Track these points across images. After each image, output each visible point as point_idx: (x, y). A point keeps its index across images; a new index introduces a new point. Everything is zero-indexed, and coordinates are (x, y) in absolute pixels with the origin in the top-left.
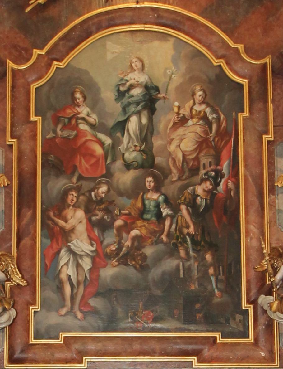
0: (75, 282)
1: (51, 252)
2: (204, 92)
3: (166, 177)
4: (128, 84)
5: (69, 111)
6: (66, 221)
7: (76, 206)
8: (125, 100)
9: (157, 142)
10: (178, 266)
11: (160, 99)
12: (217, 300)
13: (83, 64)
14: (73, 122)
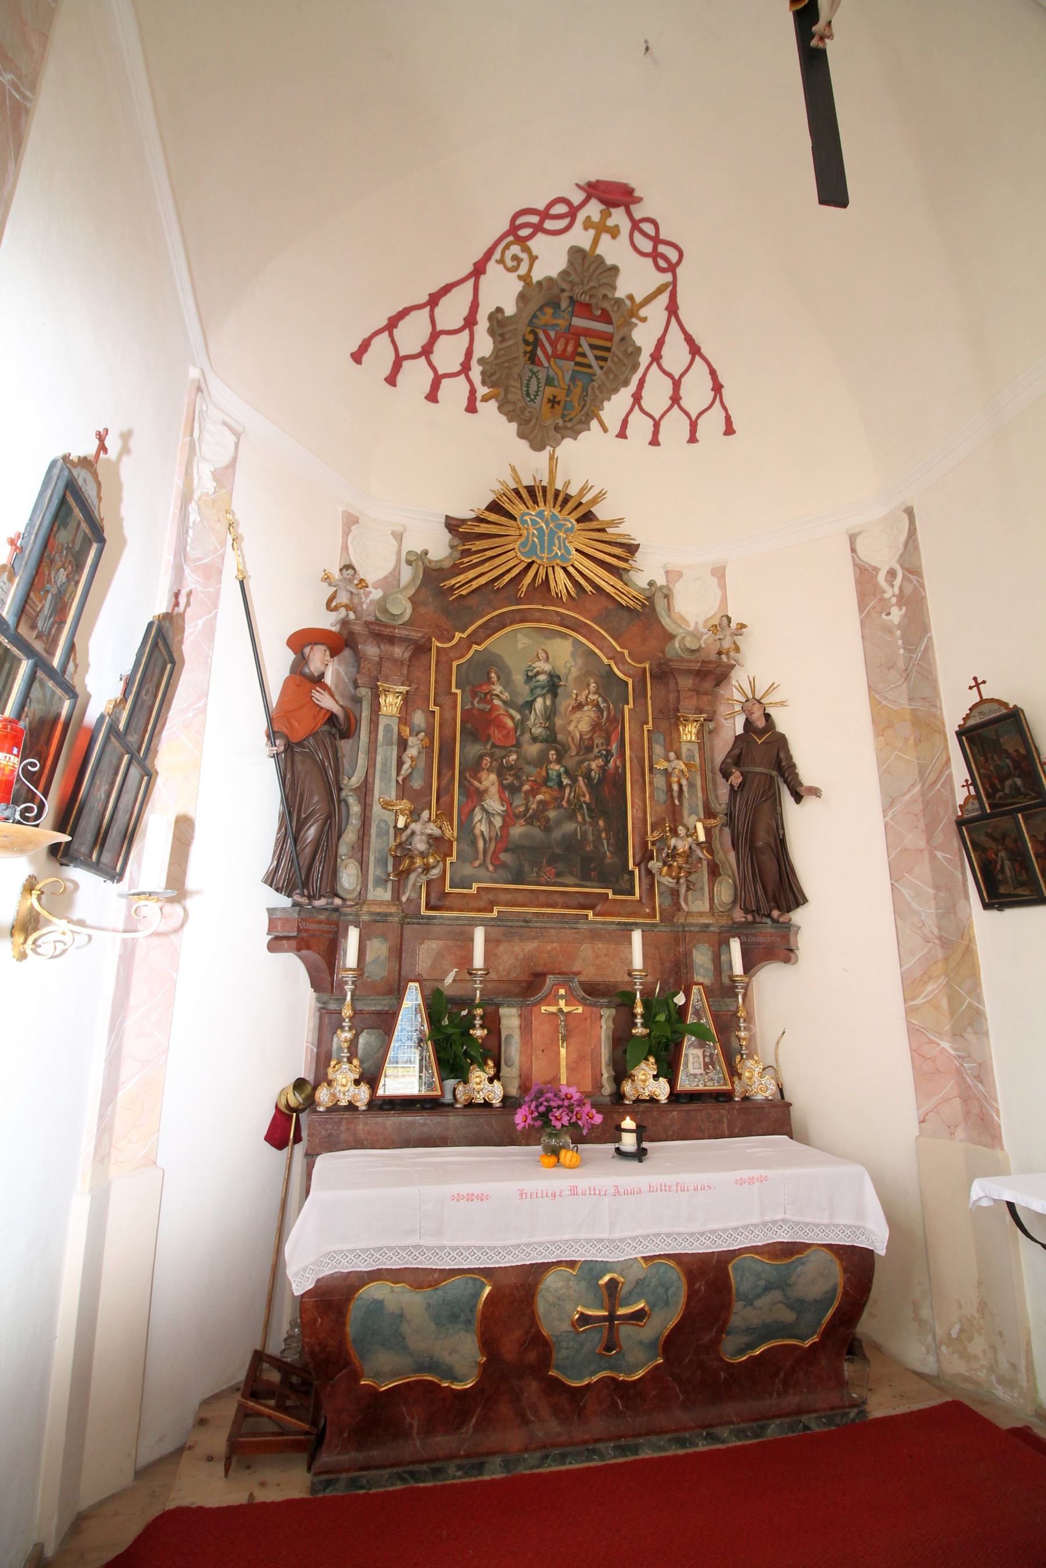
0: (487, 838)
1: (467, 809)
2: (597, 684)
3: (566, 752)
4: (535, 670)
5: (485, 688)
6: (481, 783)
7: (490, 770)
8: (533, 684)
9: (559, 722)
10: (576, 828)
11: (561, 686)
12: (608, 861)
13: (496, 650)
14: (489, 697)
